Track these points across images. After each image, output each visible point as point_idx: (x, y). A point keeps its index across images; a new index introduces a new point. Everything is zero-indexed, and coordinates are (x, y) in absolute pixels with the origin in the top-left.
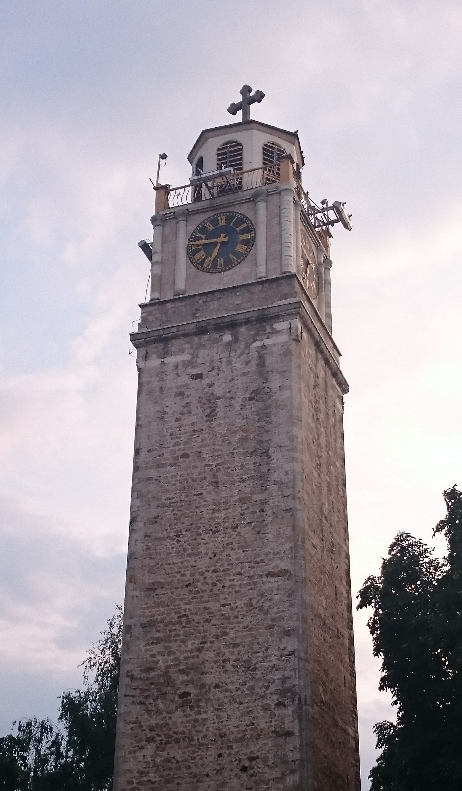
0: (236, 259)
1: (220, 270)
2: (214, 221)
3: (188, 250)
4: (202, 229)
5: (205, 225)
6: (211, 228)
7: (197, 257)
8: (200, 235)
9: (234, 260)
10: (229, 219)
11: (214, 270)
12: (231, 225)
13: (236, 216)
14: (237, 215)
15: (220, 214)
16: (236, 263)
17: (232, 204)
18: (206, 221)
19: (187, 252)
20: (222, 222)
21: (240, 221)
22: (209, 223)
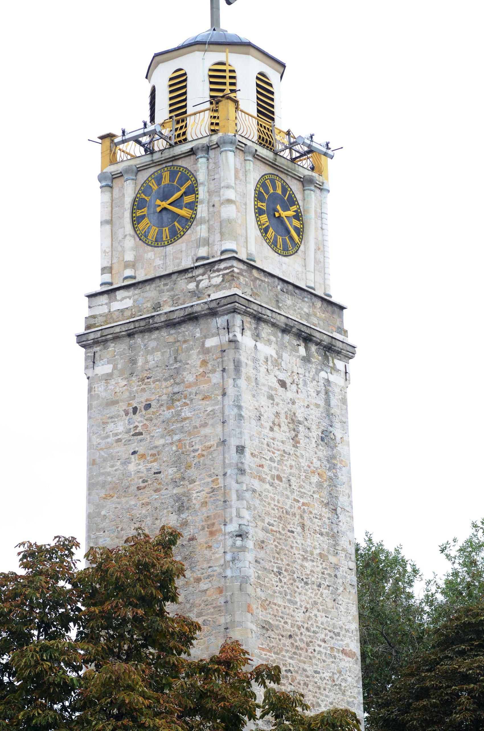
0: (181, 229)
1: (166, 243)
2: (159, 180)
3: (132, 217)
4: (145, 189)
5: (150, 184)
6: (155, 187)
7: (141, 226)
8: (144, 197)
9: (179, 229)
10: (173, 174)
11: (159, 243)
12: (175, 183)
13: (180, 171)
14: (181, 170)
15: (163, 168)
16: (182, 233)
17: (175, 158)
18: (150, 179)
19: (133, 221)
20: (166, 181)
21: (184, 178)
22: (153, 180)
